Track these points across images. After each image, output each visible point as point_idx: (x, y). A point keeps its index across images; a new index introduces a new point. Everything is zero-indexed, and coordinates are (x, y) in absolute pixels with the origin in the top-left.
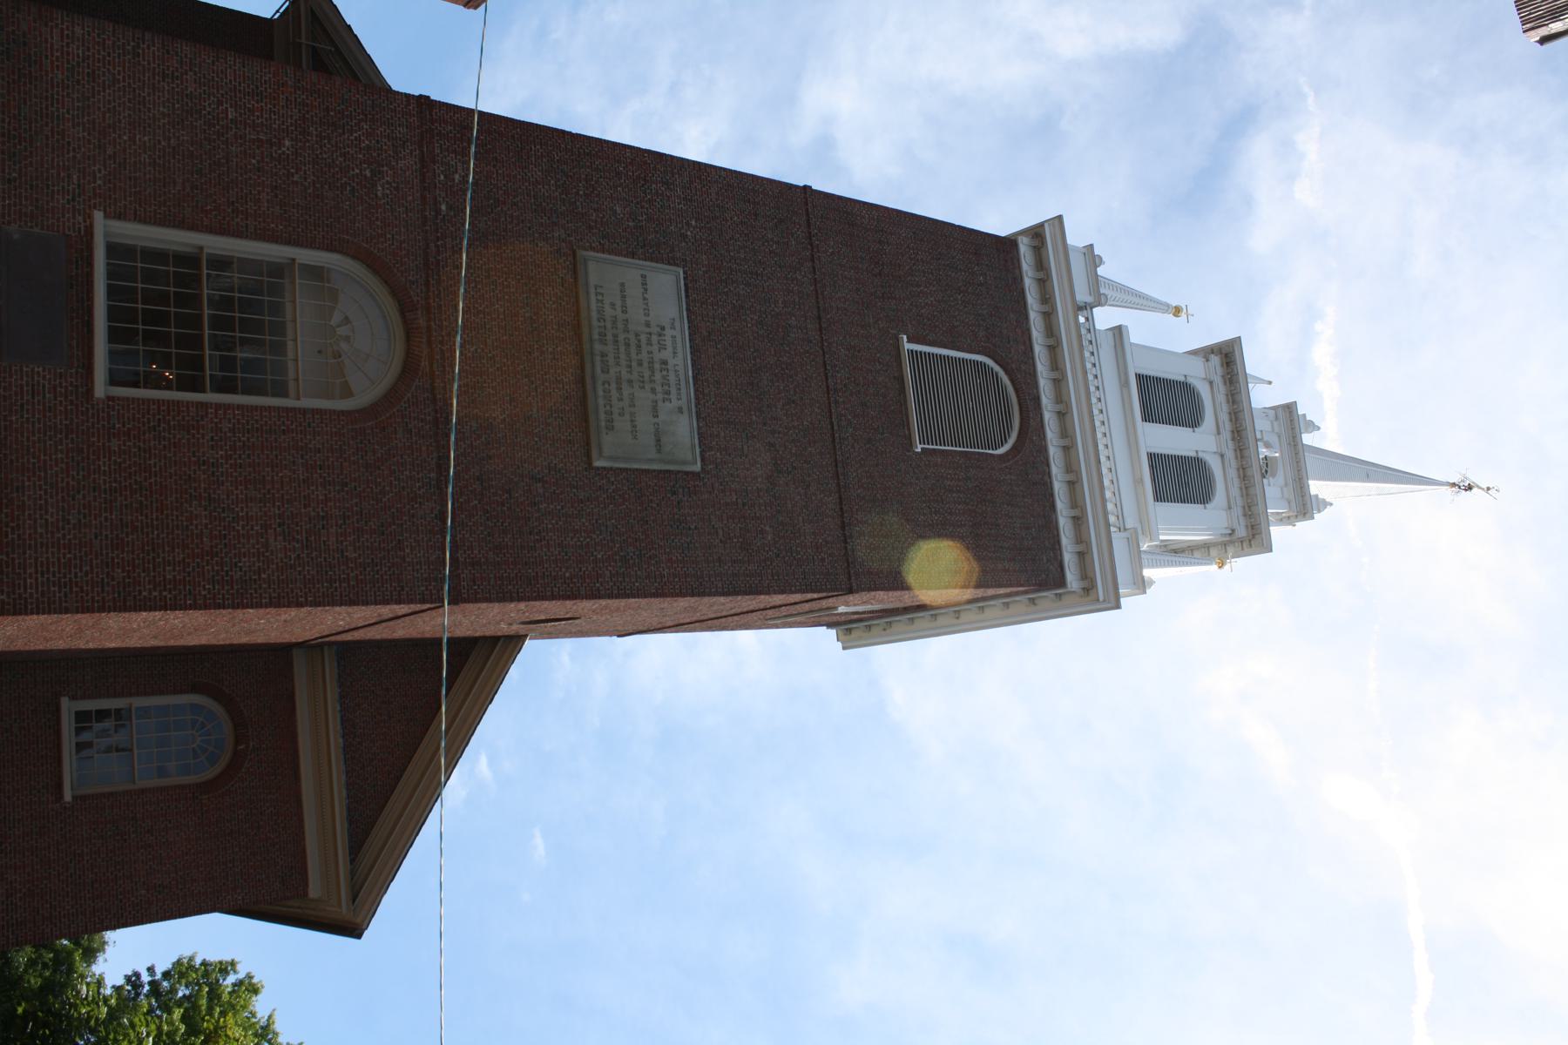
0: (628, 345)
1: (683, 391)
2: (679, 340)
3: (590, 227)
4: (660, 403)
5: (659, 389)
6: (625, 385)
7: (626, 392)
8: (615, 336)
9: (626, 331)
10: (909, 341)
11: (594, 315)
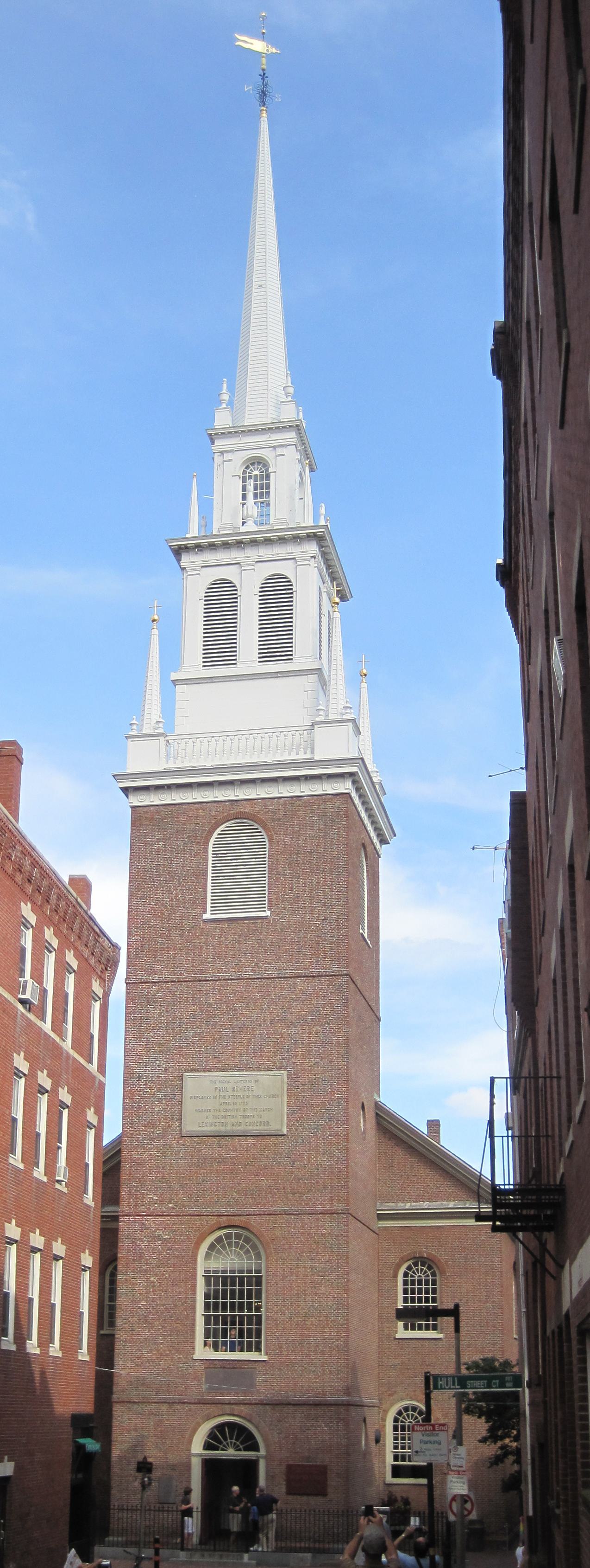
0: (227, 1110)
3: (169, 1126)
5: (247, 1093)
6: (247, 1114)
8: (223, 1117)
11: (213, 1128)
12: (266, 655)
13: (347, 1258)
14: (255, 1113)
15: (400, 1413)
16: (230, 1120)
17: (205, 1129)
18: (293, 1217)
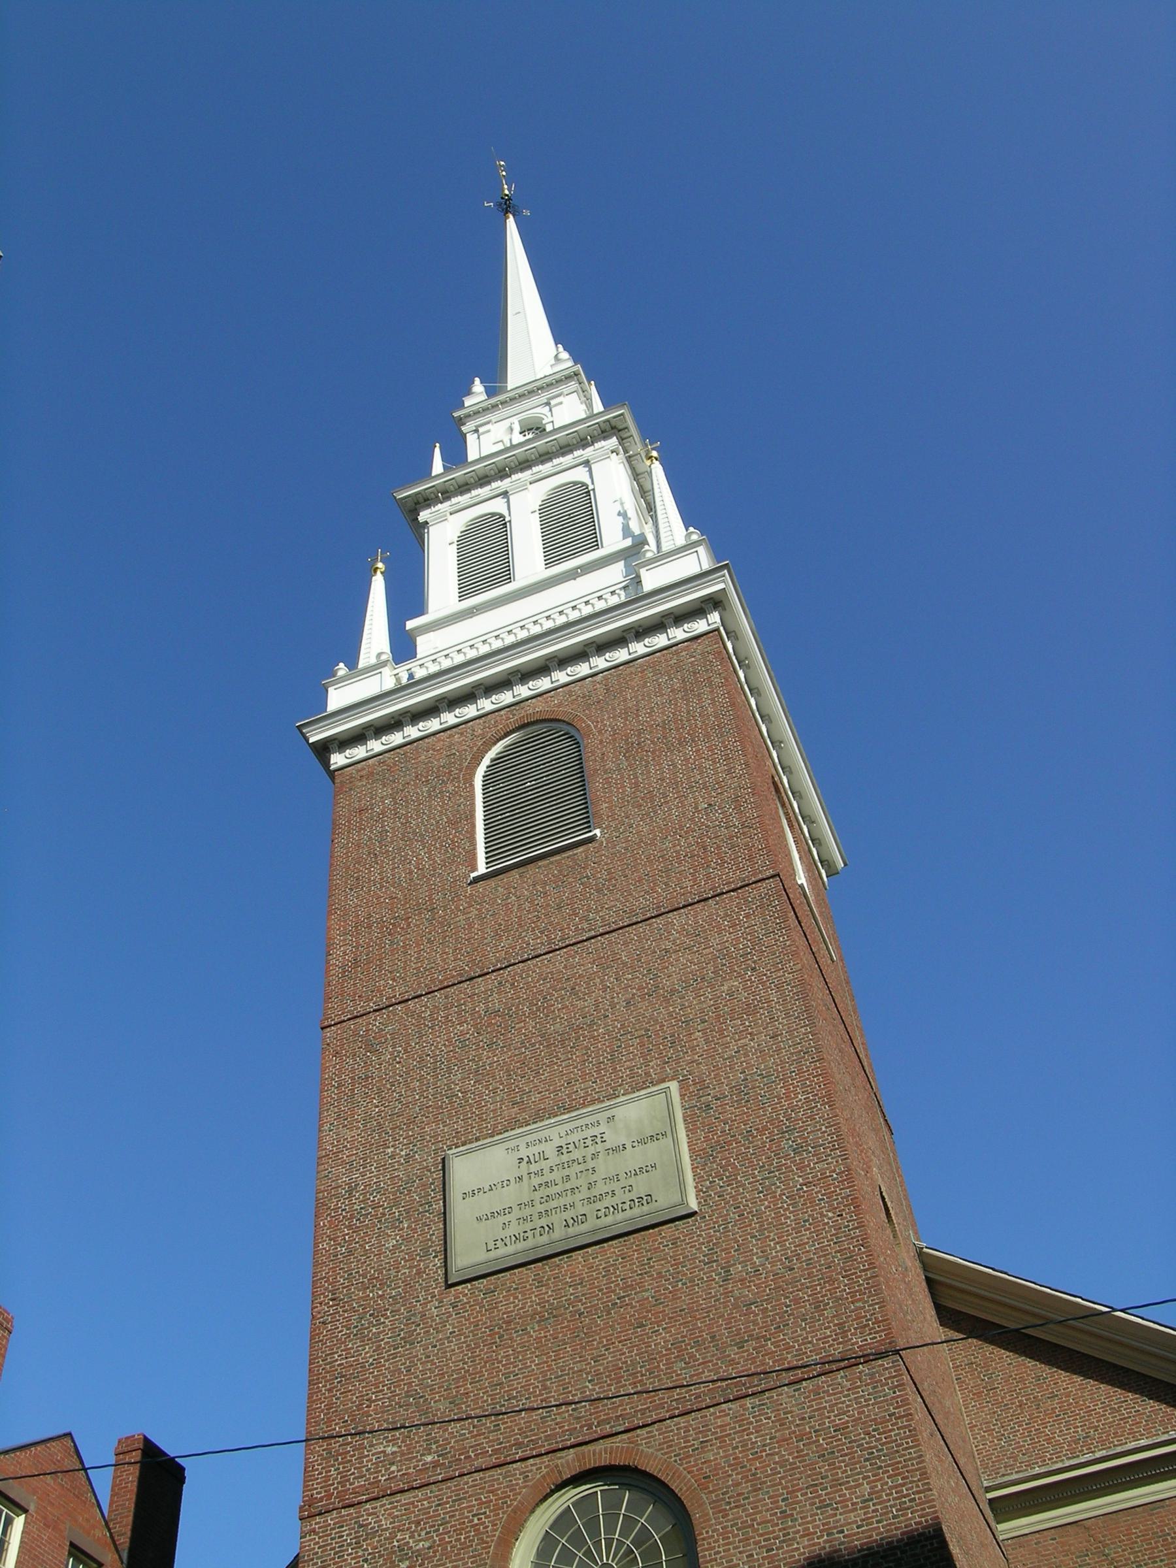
1: (588, 1120)
2: (529, 1138)
4: (608, 1145)
5: (591, 1150)
6: (596, 1192)
7: (601, 1188)
10: (474, 869)
11: (521, 1246)
13: (924, 1475)
14: (616, 1186)
16: (557, 1219)
17: (502, 1251)
18: (748, 1402)
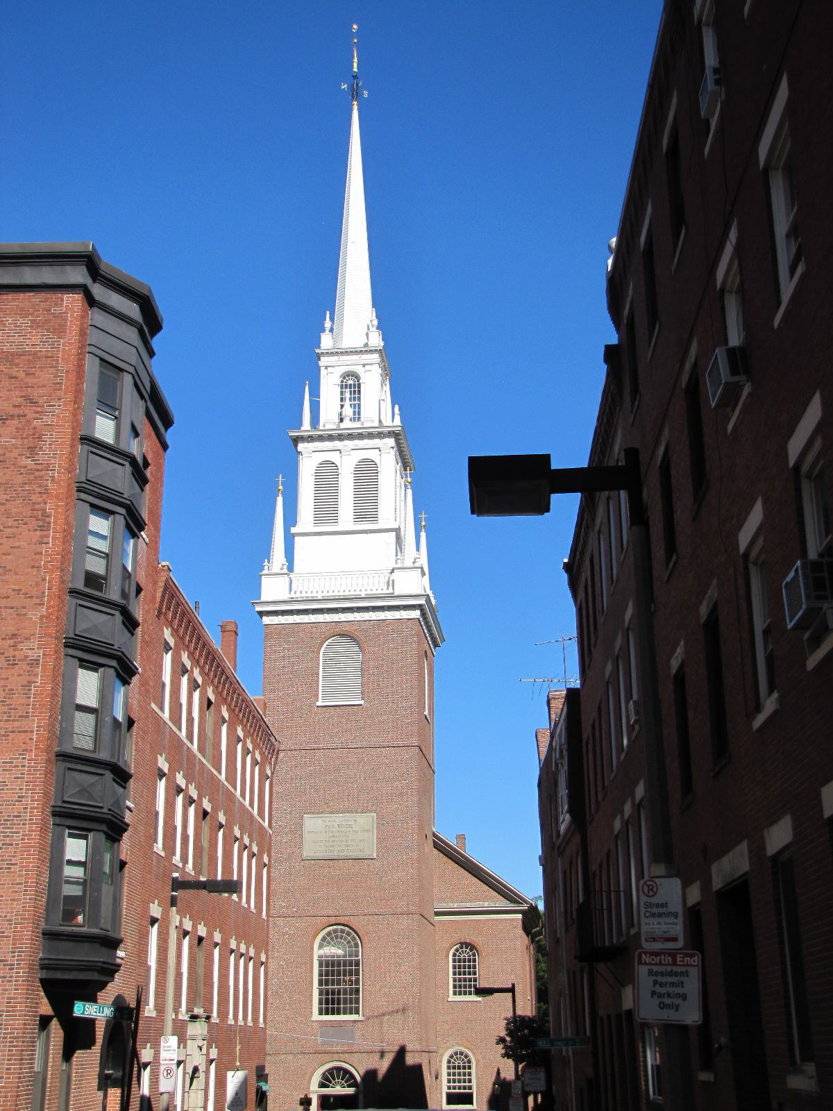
3: (293, 853)
7: (350, 843)
9: (329, 841)
12: (360, 516)
15: (451, 1057)
